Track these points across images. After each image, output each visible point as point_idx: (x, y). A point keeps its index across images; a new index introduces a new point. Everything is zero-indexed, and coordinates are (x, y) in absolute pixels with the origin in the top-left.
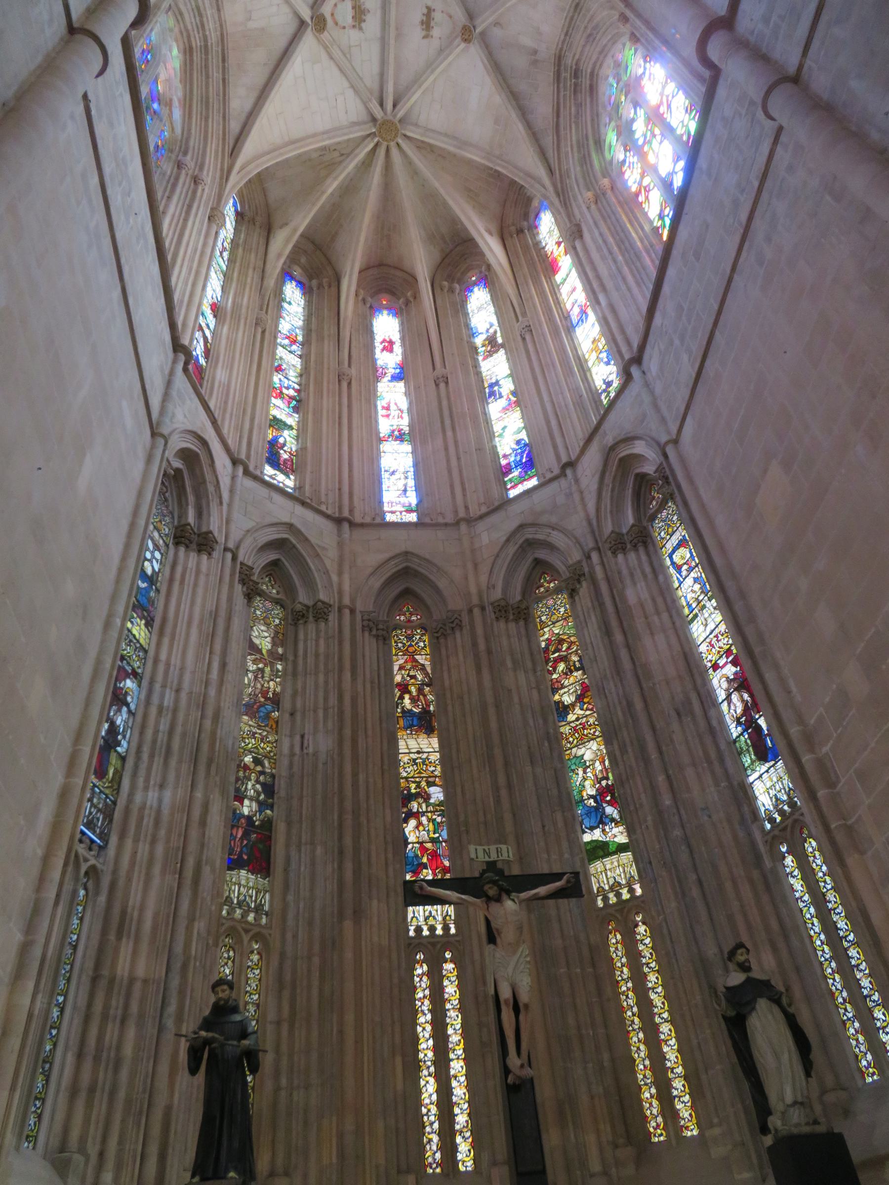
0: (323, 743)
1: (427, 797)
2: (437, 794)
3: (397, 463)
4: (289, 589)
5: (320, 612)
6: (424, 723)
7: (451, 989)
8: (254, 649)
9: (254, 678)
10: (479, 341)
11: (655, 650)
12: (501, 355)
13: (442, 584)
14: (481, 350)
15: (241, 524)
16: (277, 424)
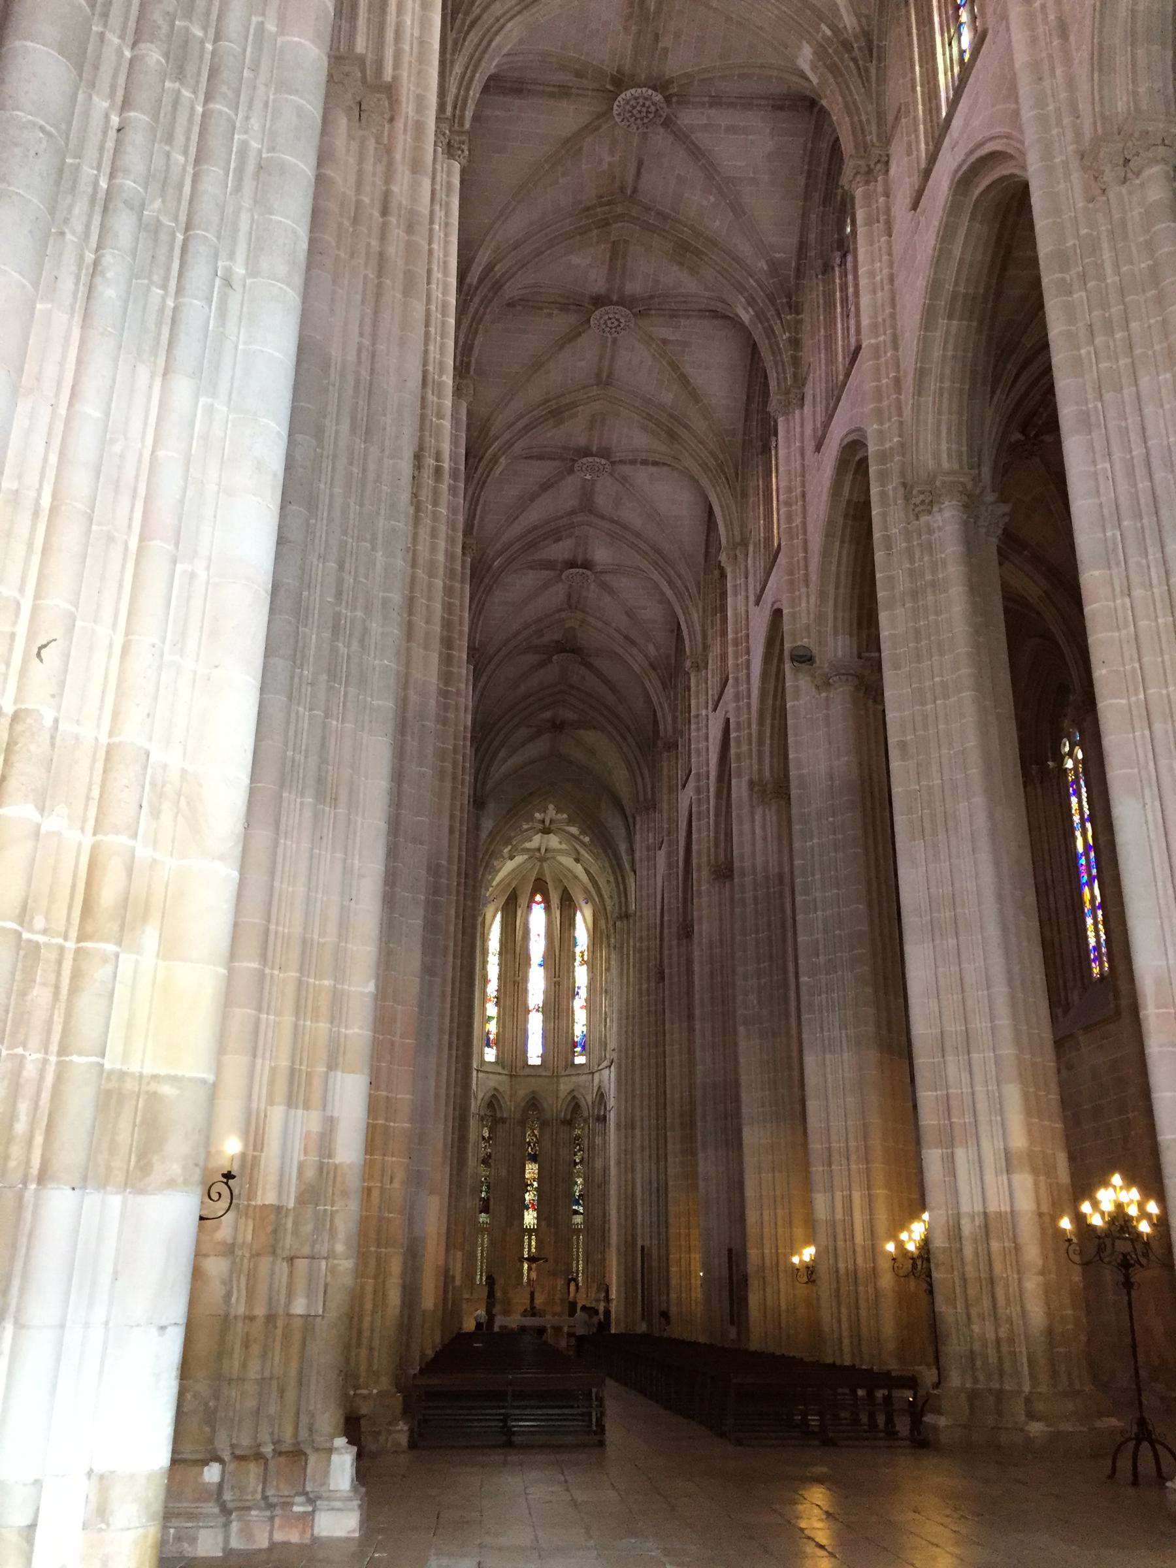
0: (504, 1173)
1: (532, 1185)
2: (536, 1184)
3: (535, 1024)
4: (495, 1110)
5: (503, 1121)
6: (534, 1158)
7: (533, 1243)
8: (484, 1138)
9: (485, 1149)
10: (578, 950)
11: (598, 1164)
12: (585, 967)
13: (545, 1105)
14: (578, 959)
15: (480, 1096)
16: (490, 1018)
